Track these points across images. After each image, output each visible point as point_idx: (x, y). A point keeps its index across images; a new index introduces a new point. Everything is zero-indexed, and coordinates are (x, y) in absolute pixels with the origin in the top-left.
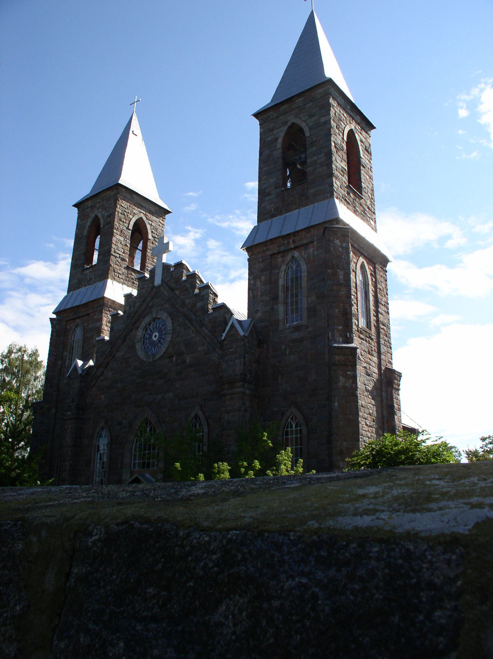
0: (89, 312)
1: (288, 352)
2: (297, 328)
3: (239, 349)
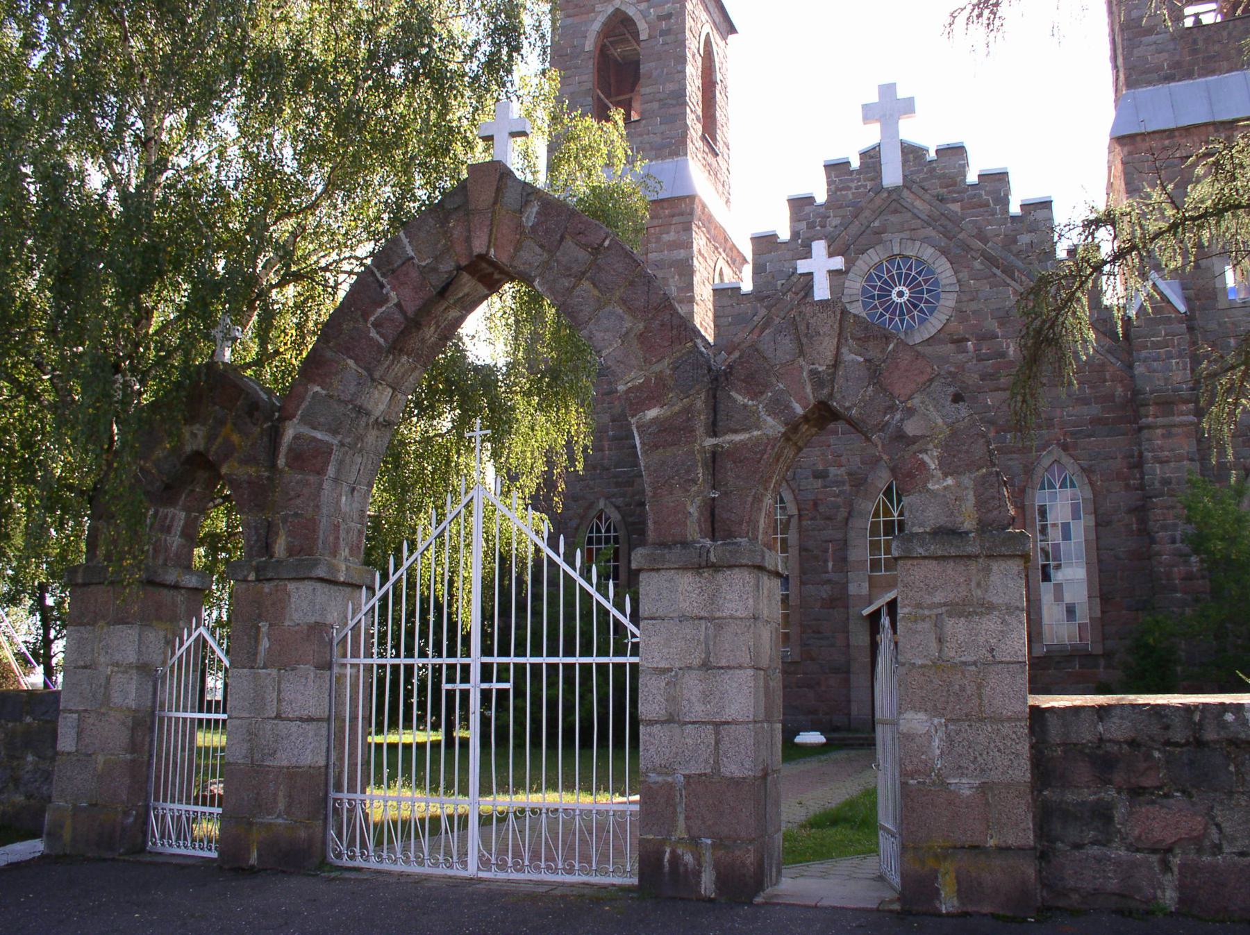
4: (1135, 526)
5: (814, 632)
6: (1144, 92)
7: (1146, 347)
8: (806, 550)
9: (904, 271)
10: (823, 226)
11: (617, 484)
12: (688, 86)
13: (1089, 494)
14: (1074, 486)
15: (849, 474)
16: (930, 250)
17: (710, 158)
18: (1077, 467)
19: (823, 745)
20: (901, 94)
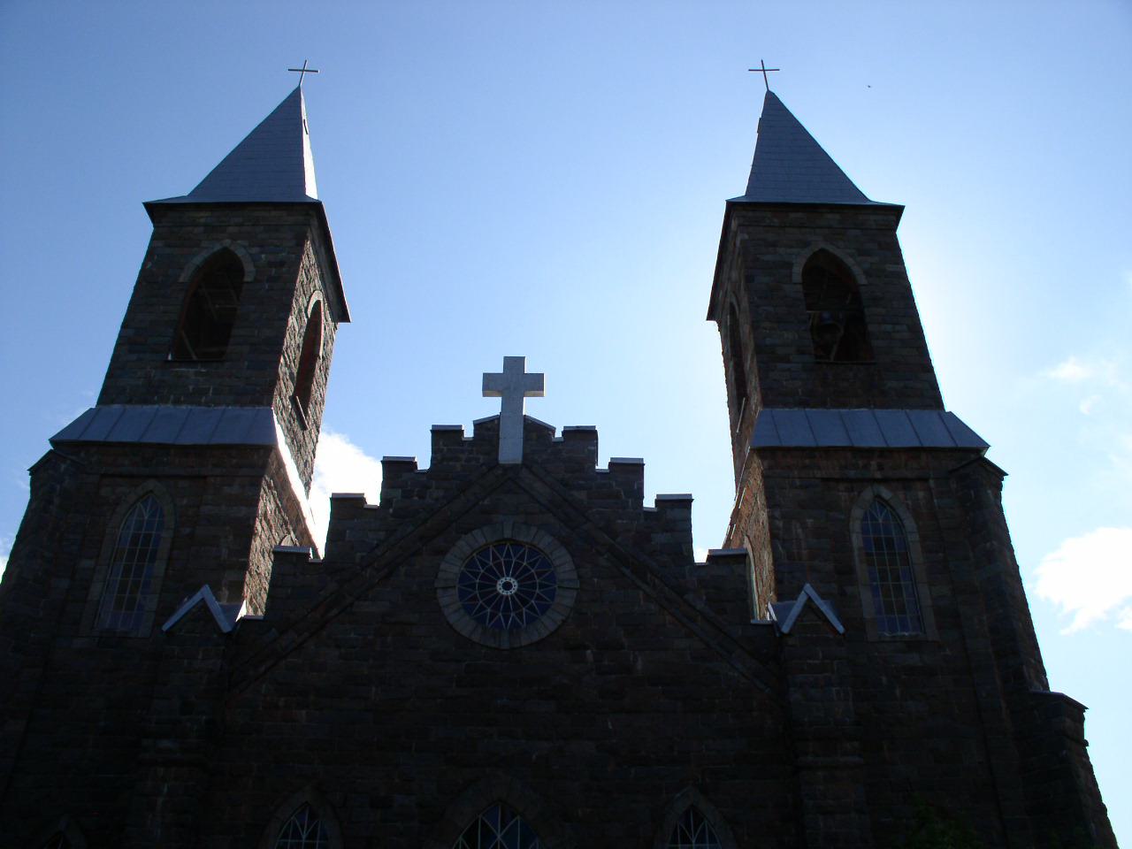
1: (898, 692)
2: (913, 645)
6: (781, 412)
10: (422, 497)
12: (287, 336)
16: (548, 539)
17: (296, 425)
20: (529, 368)
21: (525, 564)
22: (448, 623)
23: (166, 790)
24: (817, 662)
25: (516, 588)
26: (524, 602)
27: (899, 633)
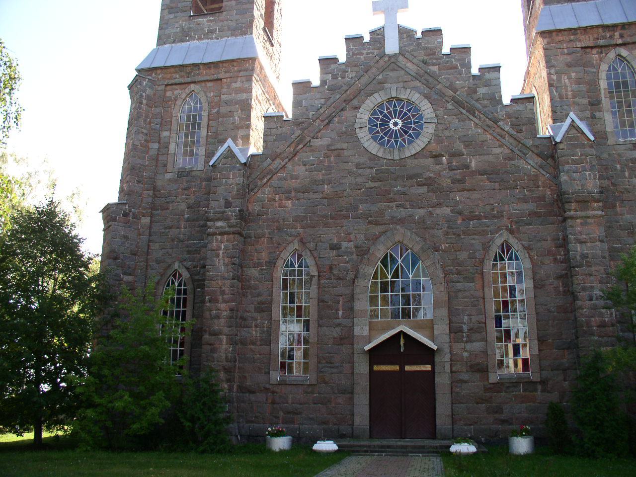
0: (220, 76)
1: (627, 174)
3: (588, 157)
4: (561, 288)
5: (327, 362)
6: (555, 8)
7: (568, 163)
8: (323, 301)
9: (398, 109)
11: (189, 252)
13: (529, 265)
14: (518, 260)
15: (356, 247)
16: (417, 95)
18: (520, 246)
19: (336, 452)
21: (405, 111)
22: (364, 147)
23: (223, 247)
24: (577, 158)
25: (401, 125)
26: (406, 133)
27: (629, 139)
